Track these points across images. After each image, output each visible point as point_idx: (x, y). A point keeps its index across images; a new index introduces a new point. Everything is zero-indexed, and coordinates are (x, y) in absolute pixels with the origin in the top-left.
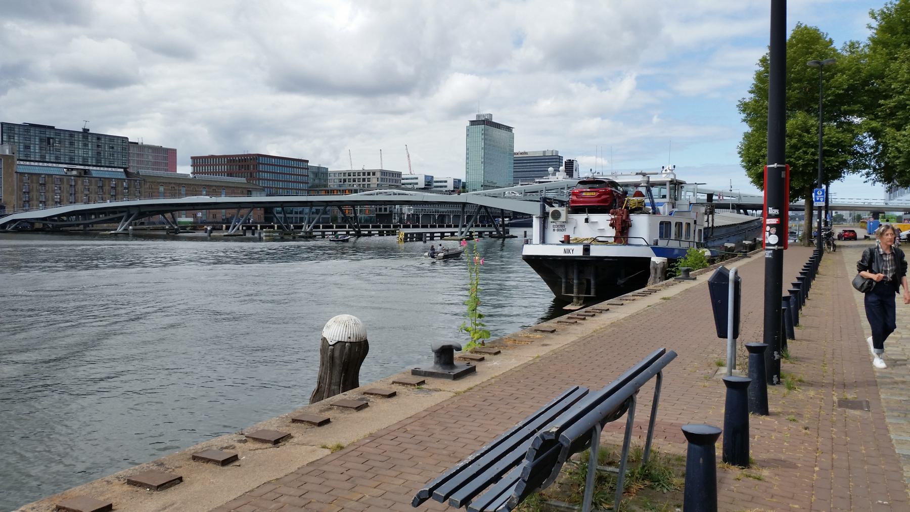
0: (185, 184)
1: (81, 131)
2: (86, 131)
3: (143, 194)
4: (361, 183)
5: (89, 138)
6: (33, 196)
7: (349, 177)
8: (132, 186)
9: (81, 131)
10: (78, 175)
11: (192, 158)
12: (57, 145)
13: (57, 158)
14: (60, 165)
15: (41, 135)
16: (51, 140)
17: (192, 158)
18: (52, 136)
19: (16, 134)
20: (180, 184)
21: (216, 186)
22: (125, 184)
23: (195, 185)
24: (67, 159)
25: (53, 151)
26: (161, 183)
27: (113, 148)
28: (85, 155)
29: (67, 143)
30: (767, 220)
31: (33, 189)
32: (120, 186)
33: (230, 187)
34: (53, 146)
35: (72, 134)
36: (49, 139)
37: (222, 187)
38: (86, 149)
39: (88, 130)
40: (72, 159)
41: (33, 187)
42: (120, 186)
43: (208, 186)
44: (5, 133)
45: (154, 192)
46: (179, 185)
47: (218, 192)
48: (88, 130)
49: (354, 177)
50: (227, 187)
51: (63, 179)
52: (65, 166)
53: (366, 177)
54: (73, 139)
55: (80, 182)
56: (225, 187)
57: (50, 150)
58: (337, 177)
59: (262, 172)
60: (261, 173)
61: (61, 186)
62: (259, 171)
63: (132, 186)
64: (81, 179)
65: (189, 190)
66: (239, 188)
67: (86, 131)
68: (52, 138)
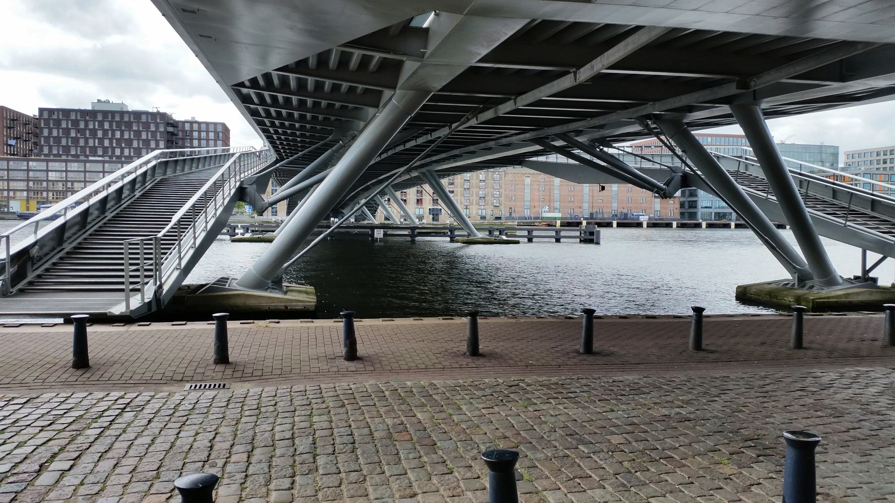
3: (503, 186)
4: (882, 166)
7: (878, 158)
30: (116, 154)
45: (518, 184)
49: (885, 157)
53: (888, 157)
58: (875, 157)
61: (500, 182)
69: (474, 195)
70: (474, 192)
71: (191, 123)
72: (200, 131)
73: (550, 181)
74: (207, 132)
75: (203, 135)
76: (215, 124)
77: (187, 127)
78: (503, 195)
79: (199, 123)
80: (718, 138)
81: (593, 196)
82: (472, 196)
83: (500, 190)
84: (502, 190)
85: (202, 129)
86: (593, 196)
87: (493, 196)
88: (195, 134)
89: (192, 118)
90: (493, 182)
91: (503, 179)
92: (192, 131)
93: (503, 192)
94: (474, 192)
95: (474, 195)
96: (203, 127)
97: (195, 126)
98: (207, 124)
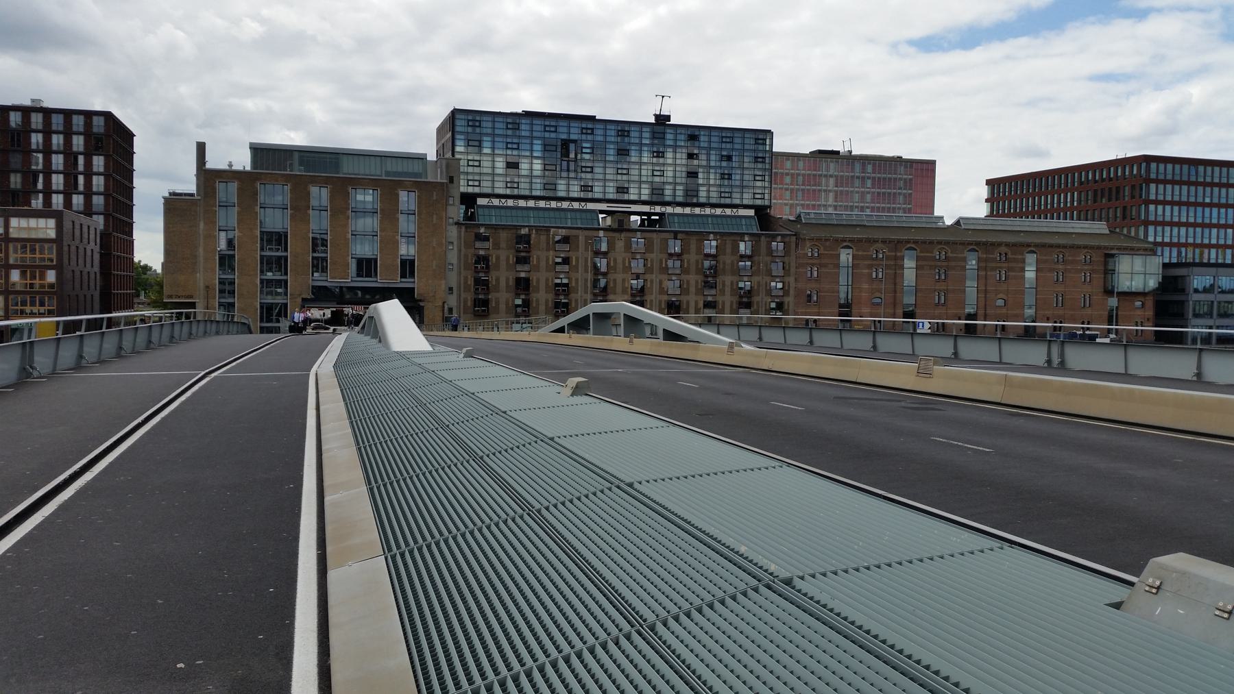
0: (916, 242)
1: (653, 121)
2: (662, 119)
3: (793, 270)
5: (669, 136)
6: (498, 280)
8: (763, 249)
9: (653, 121)
10: (616, 226)
11: (989, 182)
12: (587, 157)
13: (586, 188)
14: (591, 206)
15: (547, 135)
16: (572, 147)
17: (989, 182)
18: (573, 137)
19: (487, 135)
20: (899, 242)
21: (1007, 245)
22: (742, 246)
23: (947, 243)
24: (611, 190)
25: (575, 171)
26: (844, 240)
27: (729, 158)
28: (657, 179)
29: (612, 152)
31: (615, 268)
32: (729, 250)
33: (1051, 246)
34: (576, 160)
35: (624, 128)
36: (565, 144)
37: (1029, 245)
38: (658, 164)
39: (668, 118)
40: (622, 190)
41: (498, 258)
42: (729, 250)
43: (985, 244)
44: (461, 133)
45: (825, 266)
46: (897, 245)
47: (1015, 260)
48: (668, 118)
50: (1043, 246)
51: (577, 237)
52: (603, 206)
54: (626, 139)
55: (620, 245)
56: (1036, 246)
57: (568, 170)
59: (1156, 202)
60: (1152, 207)
62: (1148, 202)
63: (763, 249)
64: (623, 235)
65: (924, 259)
66: (1079, 247)
67: (662, 119)
68: (575, 141)
69: (728, 289)
70: (728, 283)
71: (26, 111)
72: (47, 132)
73: (896, 258)
74: (68, 134)
75: (57, 140)
76: (89, 115)
77: (15, 119)
78: (792, 292)
79: (48, 113)
80: (1217, 169)
81: (986, 291)
82: (723, 292)
83: (786, 279)
84: (791, 279)
85: (54, 128)
86: (986, 291)
87: (769, 291)
88: (36, 139)
89: (33, 101)
90: (769, 259)
91: (793, 252)
92: (26, 130)
93: (793, 285)
94: (728, 283)
95: (728, 289)
96: (58, 122)
97: (37, 120)
98: (68, 114)
